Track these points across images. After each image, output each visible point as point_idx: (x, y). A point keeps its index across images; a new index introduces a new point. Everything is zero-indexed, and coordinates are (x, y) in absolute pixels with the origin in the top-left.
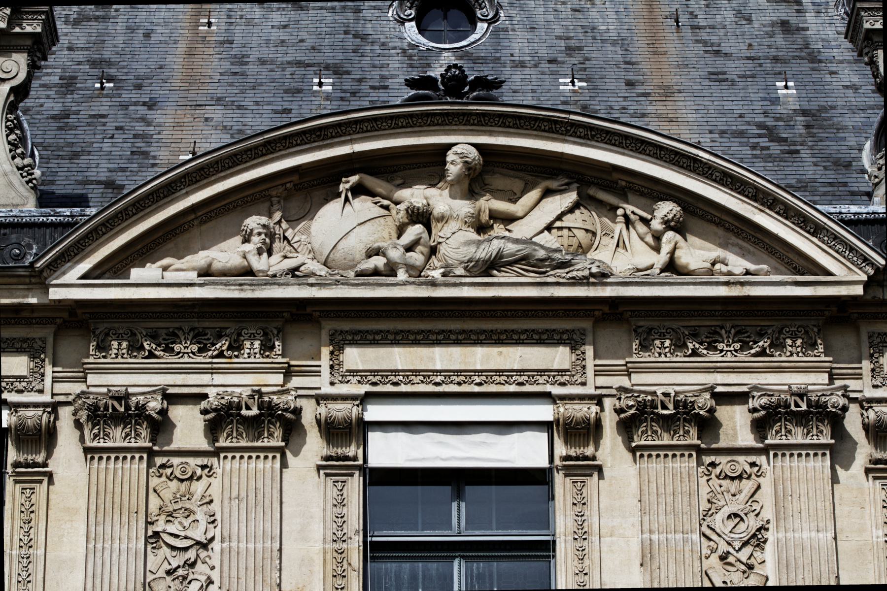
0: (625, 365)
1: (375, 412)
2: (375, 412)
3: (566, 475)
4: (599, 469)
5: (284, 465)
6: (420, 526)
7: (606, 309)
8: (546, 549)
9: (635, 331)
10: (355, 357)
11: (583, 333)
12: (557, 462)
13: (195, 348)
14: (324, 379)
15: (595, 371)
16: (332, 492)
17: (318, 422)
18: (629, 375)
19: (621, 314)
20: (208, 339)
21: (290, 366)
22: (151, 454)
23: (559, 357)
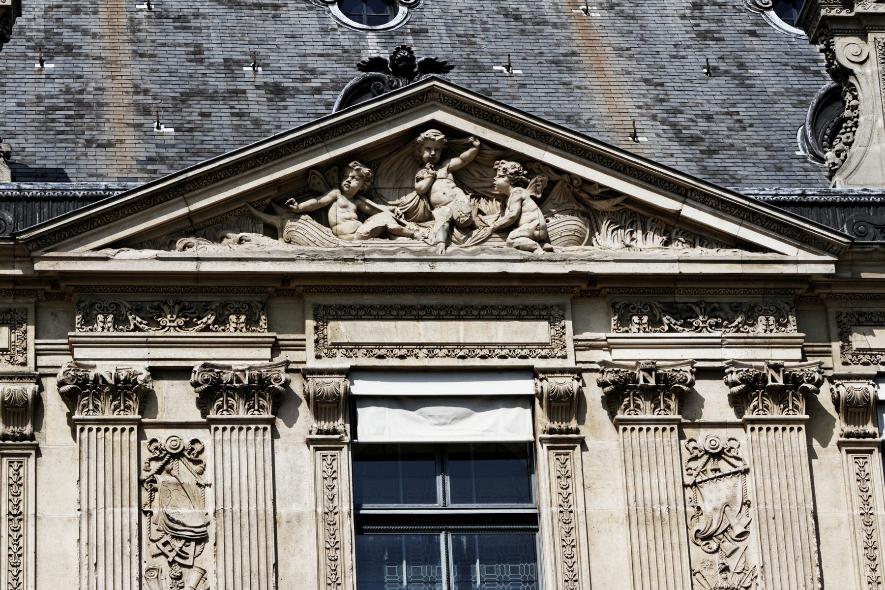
0: (606, 340)
1: (361, 387)
2: (361, 387)
3: (549, 448)
4: (582, 442)
5: (275, 435)
6: (402, 500)
7: (584, 286)
8: (533, 519)
9: (613, 307)
10: (344, 330)
11: (561, 307)
12: (540, 435)
13: (181, 321)
14: (318, 351)
15: (575, 346)
16: (321, 465)
17: (307, 396)
18: (610, 351)
19: (599, 291)
20: (195, 313)
21: (277, 340)
22: (142, 427)
23: (538, 331)
